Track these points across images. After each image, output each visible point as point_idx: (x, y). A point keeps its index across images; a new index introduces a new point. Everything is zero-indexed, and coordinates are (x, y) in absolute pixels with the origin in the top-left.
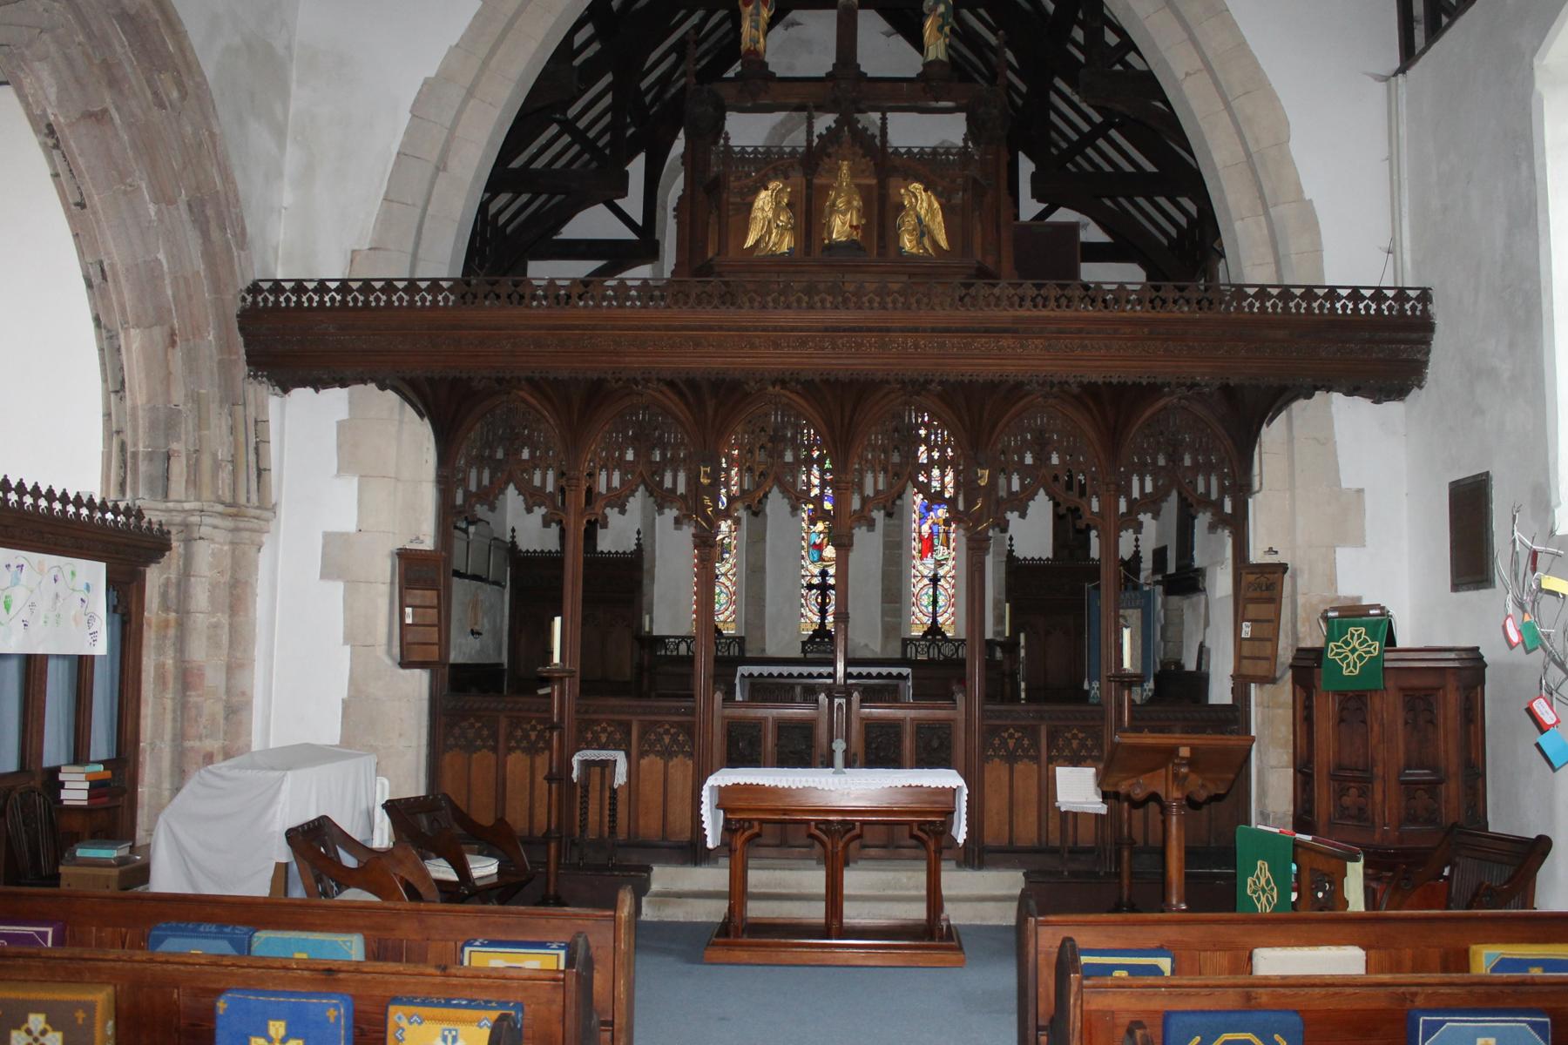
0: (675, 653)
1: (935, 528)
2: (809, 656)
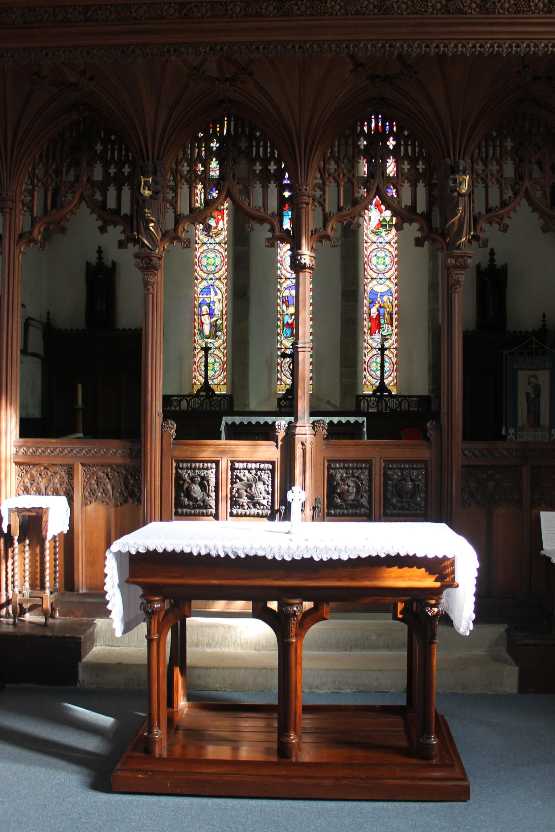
0: (177, 409)
1: (382, 311)
2: (283, 410)
